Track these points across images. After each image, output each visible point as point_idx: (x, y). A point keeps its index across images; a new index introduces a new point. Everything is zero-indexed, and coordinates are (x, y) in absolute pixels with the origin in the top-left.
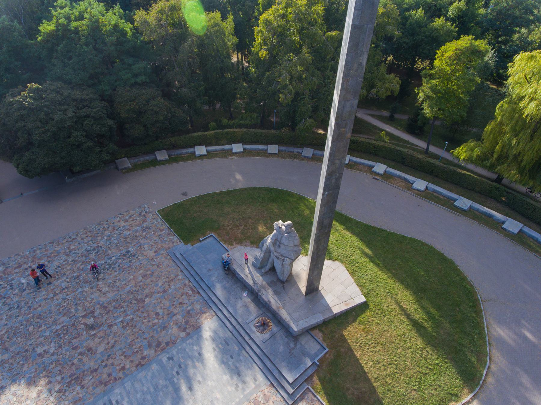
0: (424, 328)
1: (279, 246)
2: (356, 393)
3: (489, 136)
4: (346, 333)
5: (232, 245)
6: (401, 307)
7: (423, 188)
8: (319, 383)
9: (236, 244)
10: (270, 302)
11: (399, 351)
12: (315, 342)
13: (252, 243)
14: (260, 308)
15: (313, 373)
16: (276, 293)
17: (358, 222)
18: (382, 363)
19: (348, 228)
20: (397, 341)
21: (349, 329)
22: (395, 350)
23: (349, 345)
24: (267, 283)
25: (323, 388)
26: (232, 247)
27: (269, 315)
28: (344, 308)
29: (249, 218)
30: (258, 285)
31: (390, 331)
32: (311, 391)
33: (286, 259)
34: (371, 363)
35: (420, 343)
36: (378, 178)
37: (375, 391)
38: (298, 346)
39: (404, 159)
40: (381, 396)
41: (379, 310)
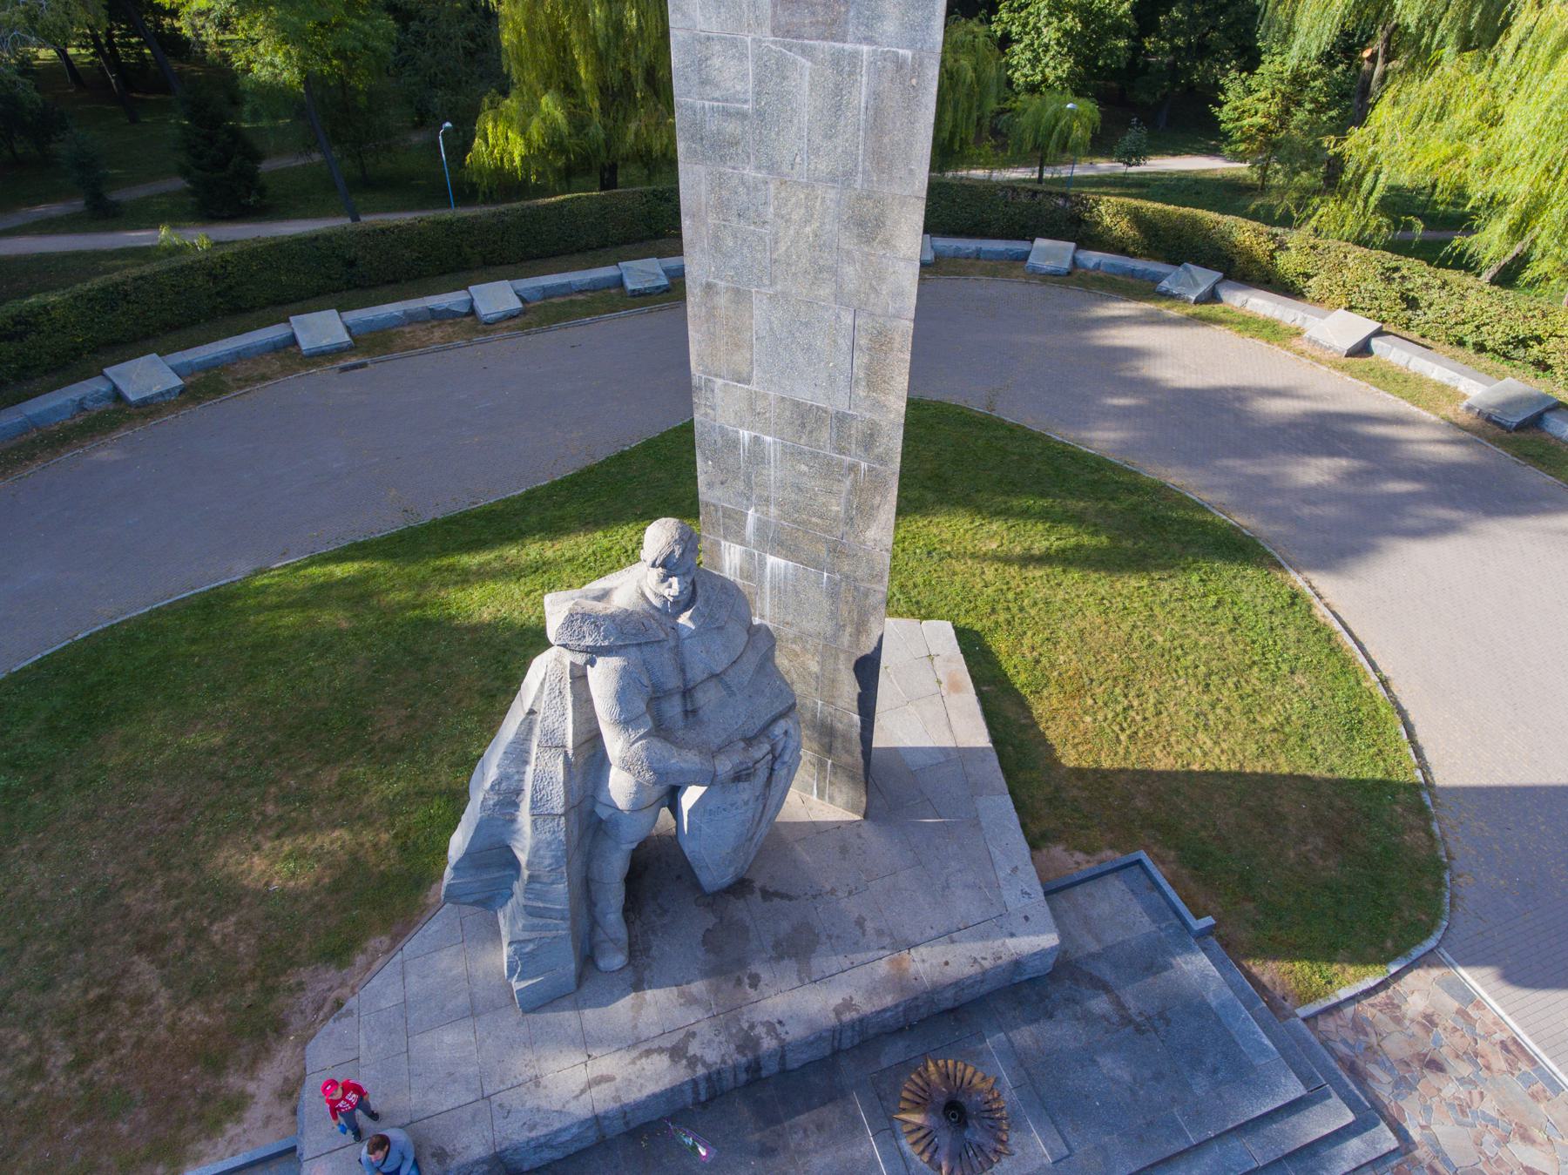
0: (1078, 547)
1: (691, 713)
2: (1320, 842)
3: (534, 51)
4: (1070, 758)
5: (236, 1106)
6: (996, 558)
7: (516, 304)
8: (1286, 966)
9: (251, 1070)
10: (848, 1005)
11: (1160, 639)
12: (1090, 887)
13: (339, 953)
14: (834, 1095)
15: (1240, 966)
16: (798, 948)
17: (530, 496)
18: (1206, 707)
19: (553, 529)
20: (1126, 627)
21: (1053, 734)
22: (1156, 650)
23: (1122, 771)
24: (706, 974)
25: (1312, 959)
26: (255, 1114)
27: (893, 1053)
28: (968, 699)
29: (105, 896)
30: (705, 1029)
31: (1083, 624)
32: (1315, 1016)
33: (778, 730)
34: (1201, 736)
35: (1132, 582)
36: (354, 361)
37: (1305, 778)
38: (1105, 972)
39: (351, 264)
40: (1319, 772)
41: (993, 611)
